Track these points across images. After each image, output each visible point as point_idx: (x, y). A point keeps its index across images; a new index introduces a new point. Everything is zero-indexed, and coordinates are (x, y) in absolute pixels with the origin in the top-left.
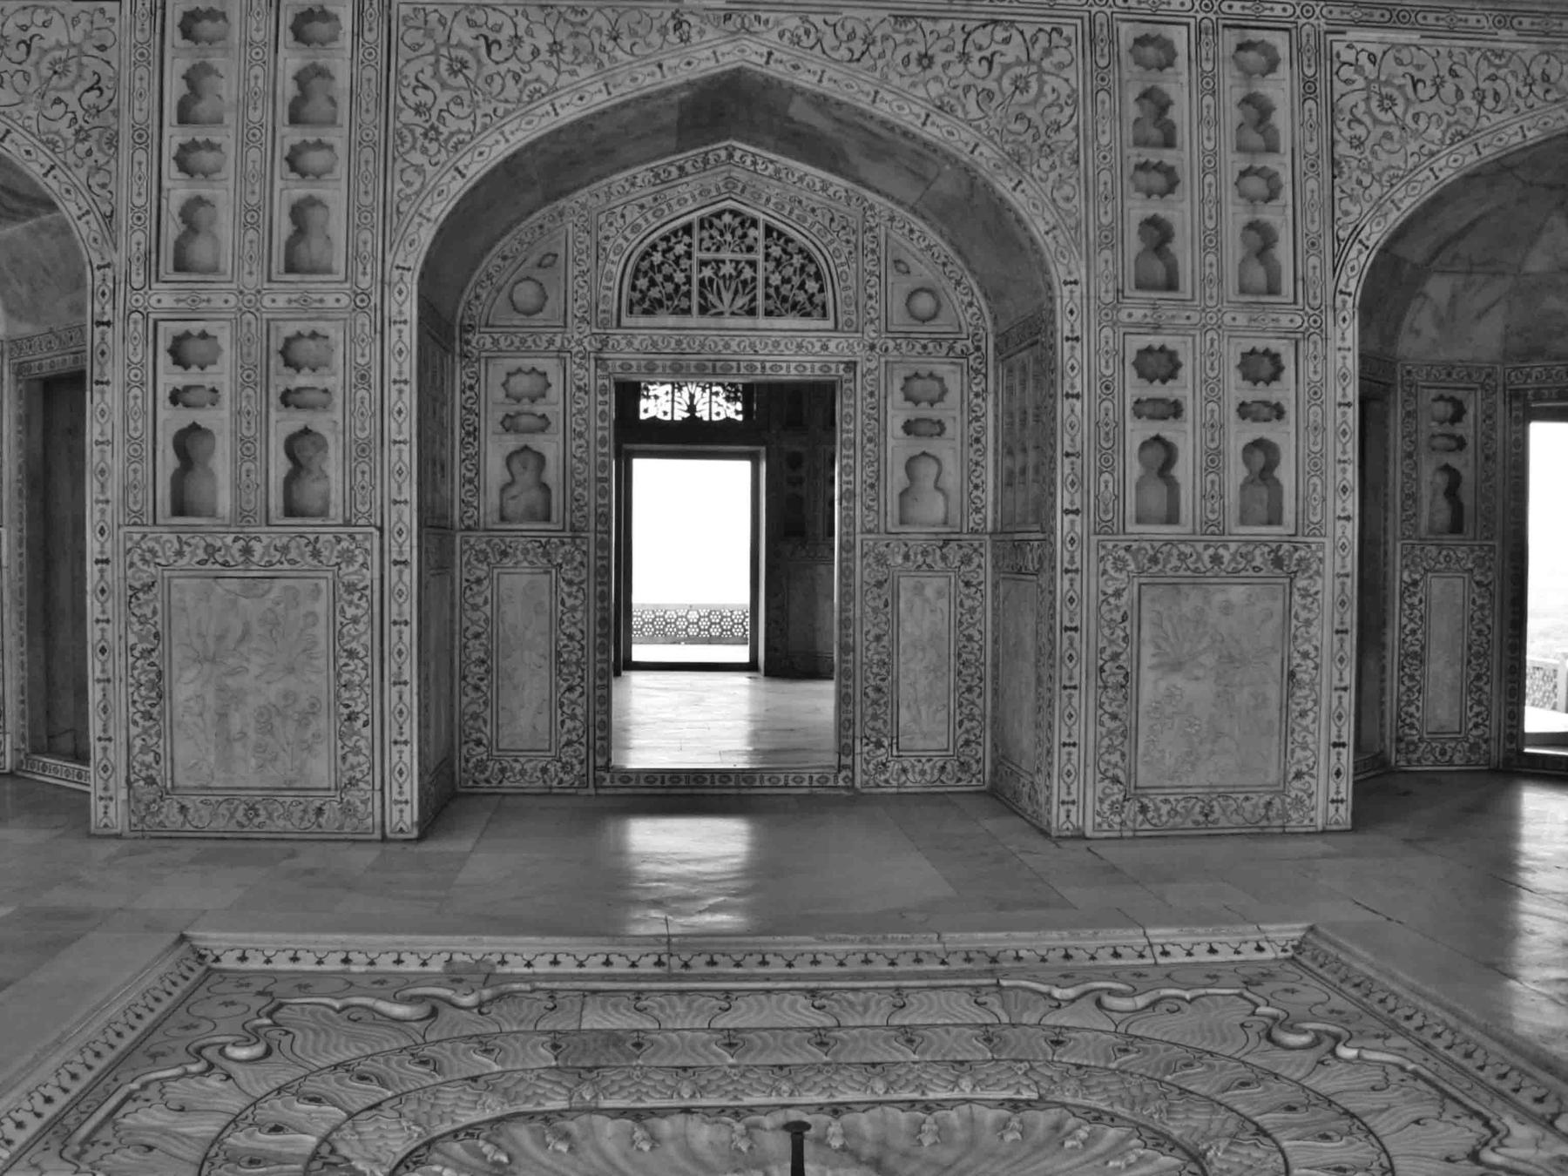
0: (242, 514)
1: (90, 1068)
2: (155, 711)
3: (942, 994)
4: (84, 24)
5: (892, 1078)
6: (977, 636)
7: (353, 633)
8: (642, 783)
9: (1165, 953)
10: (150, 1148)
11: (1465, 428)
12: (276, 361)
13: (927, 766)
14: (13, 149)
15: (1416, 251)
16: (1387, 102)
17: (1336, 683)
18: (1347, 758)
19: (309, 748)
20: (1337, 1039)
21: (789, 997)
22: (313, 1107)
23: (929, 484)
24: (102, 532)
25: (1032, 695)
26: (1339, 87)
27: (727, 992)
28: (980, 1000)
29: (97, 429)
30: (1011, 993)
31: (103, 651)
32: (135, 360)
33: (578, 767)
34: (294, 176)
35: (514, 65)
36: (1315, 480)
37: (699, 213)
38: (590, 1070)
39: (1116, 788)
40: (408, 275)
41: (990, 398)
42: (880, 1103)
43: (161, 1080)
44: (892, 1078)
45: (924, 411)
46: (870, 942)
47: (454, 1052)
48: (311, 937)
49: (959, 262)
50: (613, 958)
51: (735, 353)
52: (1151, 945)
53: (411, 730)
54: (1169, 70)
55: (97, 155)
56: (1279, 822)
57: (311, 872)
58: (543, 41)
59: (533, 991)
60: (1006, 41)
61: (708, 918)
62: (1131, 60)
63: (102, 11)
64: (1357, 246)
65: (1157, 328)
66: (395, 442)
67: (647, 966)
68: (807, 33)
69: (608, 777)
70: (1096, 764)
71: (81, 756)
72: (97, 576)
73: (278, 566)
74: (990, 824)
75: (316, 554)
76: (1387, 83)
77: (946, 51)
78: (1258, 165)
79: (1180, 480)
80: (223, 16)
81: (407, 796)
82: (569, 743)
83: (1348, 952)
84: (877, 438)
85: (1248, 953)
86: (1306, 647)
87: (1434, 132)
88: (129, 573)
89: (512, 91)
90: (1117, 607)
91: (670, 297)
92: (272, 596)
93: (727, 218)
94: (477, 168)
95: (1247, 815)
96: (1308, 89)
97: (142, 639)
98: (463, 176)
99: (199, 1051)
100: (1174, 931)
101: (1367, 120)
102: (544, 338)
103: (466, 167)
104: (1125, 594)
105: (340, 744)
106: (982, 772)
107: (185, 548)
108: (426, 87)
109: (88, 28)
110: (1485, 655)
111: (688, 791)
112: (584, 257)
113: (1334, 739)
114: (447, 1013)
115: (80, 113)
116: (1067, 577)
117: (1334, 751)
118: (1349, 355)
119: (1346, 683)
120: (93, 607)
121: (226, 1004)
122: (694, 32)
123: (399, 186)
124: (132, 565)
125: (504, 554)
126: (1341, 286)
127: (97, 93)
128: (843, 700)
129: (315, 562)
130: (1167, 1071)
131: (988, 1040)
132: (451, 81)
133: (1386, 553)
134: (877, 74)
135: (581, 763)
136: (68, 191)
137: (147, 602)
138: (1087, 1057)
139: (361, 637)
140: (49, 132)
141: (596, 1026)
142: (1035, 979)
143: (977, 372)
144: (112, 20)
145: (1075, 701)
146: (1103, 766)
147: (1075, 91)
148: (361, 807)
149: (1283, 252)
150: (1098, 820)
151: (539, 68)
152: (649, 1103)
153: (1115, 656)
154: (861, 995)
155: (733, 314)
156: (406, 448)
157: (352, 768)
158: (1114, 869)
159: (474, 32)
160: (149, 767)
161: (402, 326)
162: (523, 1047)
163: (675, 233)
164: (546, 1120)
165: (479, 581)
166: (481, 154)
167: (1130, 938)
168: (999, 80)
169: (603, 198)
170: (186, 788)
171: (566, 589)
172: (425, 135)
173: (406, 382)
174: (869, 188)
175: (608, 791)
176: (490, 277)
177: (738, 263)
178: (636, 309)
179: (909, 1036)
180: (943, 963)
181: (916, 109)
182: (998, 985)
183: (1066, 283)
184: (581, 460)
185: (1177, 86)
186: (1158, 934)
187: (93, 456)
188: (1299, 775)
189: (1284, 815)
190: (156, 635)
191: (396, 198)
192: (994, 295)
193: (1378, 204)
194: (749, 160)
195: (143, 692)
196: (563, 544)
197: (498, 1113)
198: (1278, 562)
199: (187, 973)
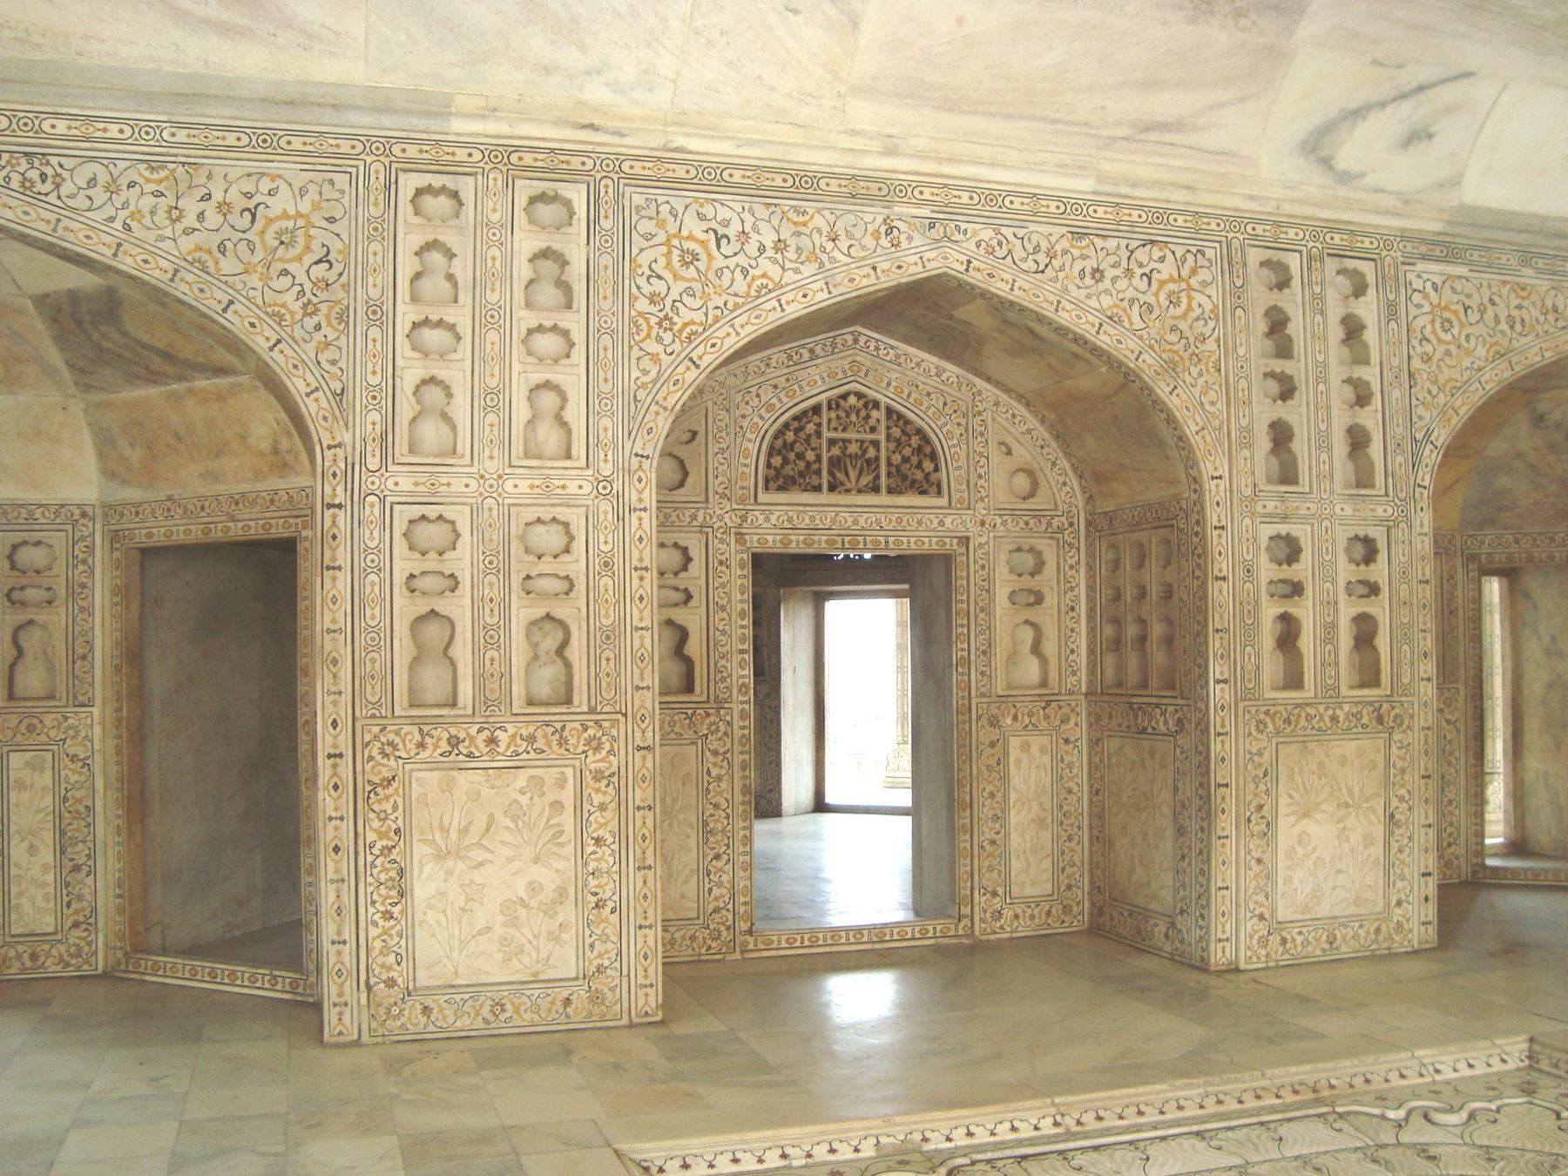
0: (485, 702)
7: (601, 820)
8: (784, 945)
13: (1036, 911)
14: (236, 322)
16: (1447, 325)
17: (1423, 821)
19: (554, 938)
24: (334, 724)
25: (1168, 845)
26: (1413, 311)
31: (336, 849)
33: (724, 933)
35: (741, 260)
37: (828, 394)
40: (646, 464)
41: (1083, 570)
48: (737, 1137)
49: (1054, 445)
51: (863, 529)
54: (1286, 291)
55: (326, 330)
58: (769, 238)
60: (1162, 259)
63: (332, 182)
65: (1285, 518)
66: (637, 629)
68: (1000, 244)
69: (751, 940)
70: (1247, 904)
72: (329, 772)
73: (524, 756)
75: (562, 742)
77: (1115, 266)
78: (1355, 376)
79: (1304, 650)
84: (988, 610)
86: (1403, 792)
87: (1481, 352)
88: (368, 767)
89: (741, 285)
90: (1260, 765)
91: (802, 474)
93: (852, 400)
94: (709, 360)
96: (1391, 311)
97: (382, 835)
98: (698, 367)
101: (1433, 339)
102: (688, 513)
103: (700, 358)
104: (1266, 753)
105: (588, 932)
106: (1082, 913)
107: (428, 740)
111: (827, 949)
112: (723, 434)
113: (1423, 870)
115: (308, 286)
116: (1219, 739)
118: (1426, 539)
122: (903, 238)
124: (371, 758)
127: (326, 265)
129: (562, 751)
132: (683, 272)
134: (1059, 285)
135: (728, 928)
136: (295, 367)
137: (387, 798)
143: (1071, 546)
144: (342, 192)
147: (1216, 306)
148: (609, 995)
149: (1375, 450)
151: (765, 265)
155: (860, 491)
156: (647, 634)
157: (600, 956)
160: (390, 969)
161: (642, 514)
163: (804, 413)
166: (713, 345)
168: (1156, 294)
169: (741, 378)
170: (428, 988)
171: (712, 759)
172: (660, 324)
173: (646, 569)
175: (752, 955)
177: (862, 442)
178: (771, 484)
181: (1091, 318)
183: (1213, 478)
184: (723, 632)
185: (1292, 302)
188: (1399, 903)
191: (633, 387)
192: (1095, 478)
193: (1443, 412)
194: (872, 345)
195: (383, 890)
196: (708, 715)
198: (1380, 720)
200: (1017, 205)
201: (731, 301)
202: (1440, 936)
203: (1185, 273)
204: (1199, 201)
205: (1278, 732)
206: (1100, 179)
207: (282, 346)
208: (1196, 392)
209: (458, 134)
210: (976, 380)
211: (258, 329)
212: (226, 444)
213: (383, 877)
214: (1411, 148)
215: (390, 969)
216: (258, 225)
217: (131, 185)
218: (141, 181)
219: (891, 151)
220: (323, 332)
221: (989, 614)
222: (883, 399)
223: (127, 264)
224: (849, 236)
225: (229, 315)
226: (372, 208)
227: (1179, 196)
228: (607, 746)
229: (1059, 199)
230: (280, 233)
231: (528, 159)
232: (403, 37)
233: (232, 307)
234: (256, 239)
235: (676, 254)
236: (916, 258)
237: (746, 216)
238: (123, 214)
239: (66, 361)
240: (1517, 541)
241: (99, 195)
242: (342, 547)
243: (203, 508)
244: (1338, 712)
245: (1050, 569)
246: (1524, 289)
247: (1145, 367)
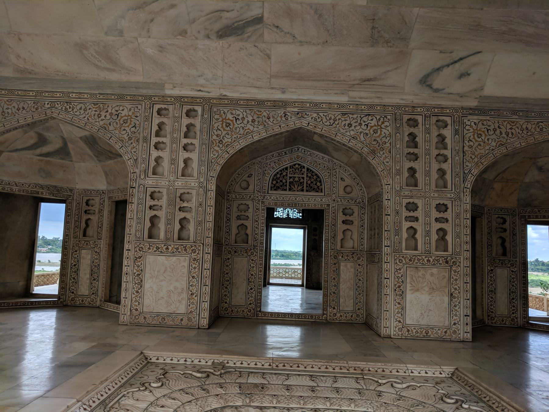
0: (167, 239)
1: (114, 387)
2: (140, 291)
3: (348, 379)
4: (132, 111)
5: (332, 402)
6: (362, 280)
9: (412, 372)
10: (128, 410)
11: (507, 226)
12: (178, 200)
14: (112, 142)
15: (490, 176)
16: (479, 136)
18: (469, 320)
19: (180, 302)
20: (463, 402)
21: (305, 377)
22: (173, 401)
23: (349, 237)
27: (288, 374)
28: (358, 381)
29: (129, 215)
30: (367, 380)
31: (127, 274)
34: (185, 151)
35: (242, 125)
36: (458, 240)
38: (249, 394)
39: (400, 324)
40: (213, 179)
41: (366, 215)
42: (328, 409)
43: (133, 392)
44: (332, 402)
45: (348, 218)
46: (328, 363)
47: (212, 387)
48: (177, 354)
50: (257, 363)
52: (408, 369)
53: (208, 298)
55: (133, 144)
56: (449, 337)
57: (177, 336)
58: (250, 119)
59: (236, 371)
60: (372, 120)
61: (284, 353)
62: (406, 125)
63: (137, 107)
64: (470, 175)
65: (411, 197)
67: (266, 366)
68: (319, 118)
70: (394, 317)
71: (118, 303)
72: (127, 254)
74: (364, 332)
75: (185, 250)
76: (480, 130)
78: (441, 153)
80: (168, 109)
81: (205, 316)
82: (250, 304)
83: (467, 376)
85: (437, 374)
86: (456, 287)
87: (494, 144)
89: (242, 131)
90: (400, 273)
91: (281, 186)
92: (173, 260)
93: (297, 166)
94: (232, 152)
95: (439, 335)
96: (456, 132)
97: (137, 271)
99: (143, 384)
100: (415, 366)
101: (473, 140)
108: (219, 130)
110: (515, 292)
113: (465, 314)
114: (212, 376)
116: (386, 264)
117: (465, 317)
118: (468, 205)
119: (468, 298)
120: (125, 262)
121: (152, 372)
122: (289, 117)
123: (212, 155)
124: (136, 251)
125: (235, 252)
126: (465, 186)
128: (325, 296)
130: (412, 406)
131: (360, 393)
132: (226, 129)
133: (482, 261)
137: (140, 261)
138: (388, 400)
139: (196, 272)
141: (252, 382)
142: (373, 376)
145: (388, 299)
146: (396, 318)
147: (390, 133)
149: (448, 177)
150: (395, 333)
152: (265, 405)
153: (399, 287)
154: (325, 378)
157: (191, 308)
158: (398, 347)
159: (232, 116)
160: (137, 306)
162: (231, 386)
163: (283, 169)
164: (236, 408)
165: (228, 259)
167: (402, 367)
168: (369, 130)
172: (219, 142)
174: (334, 158)
176: (235, 179)
179: (337, 390)
180: (348, 370)
181: (347, 138)
182: (363, 377)
184: (257, 228)
185: (419, 131)
186: (410, 366)
187: (128, 222)
188: (455, 324)
189: (451, 335)
190: (141, 270)
192: (368, 187)
193: (477, 164)
195: (137, 285)
197: (223, 405)
199: (142, 362)
200: (324, 106)
201: (239, 136)
202: (472, 337)
203: (380, 123)
204: (384, 101)
205: (407, 263)
206: (349, 97)
208: (382, 159)
210: (334, 160)
213: (137, 282)
214: (462, 79)
215: (137, 306)
217: (90, 109)
219: (284, 92)
221: (335, 226)
222: (306, 166)
224: (273, 117)
225: (111, 140)
227: (377, 101)
228: (197, 252)
229: (338, 104)
230: (124, 120)
231: (186, 100)
234: (118, 122)
235: (224, 123)
236: (293, 123)
237: (244, 113)
238: (87, 116)
240: (539, 211)
241: (82, 111)
244: (430, 259)
245: (356, 214)
246: (513, 123)
247: (364, 152)
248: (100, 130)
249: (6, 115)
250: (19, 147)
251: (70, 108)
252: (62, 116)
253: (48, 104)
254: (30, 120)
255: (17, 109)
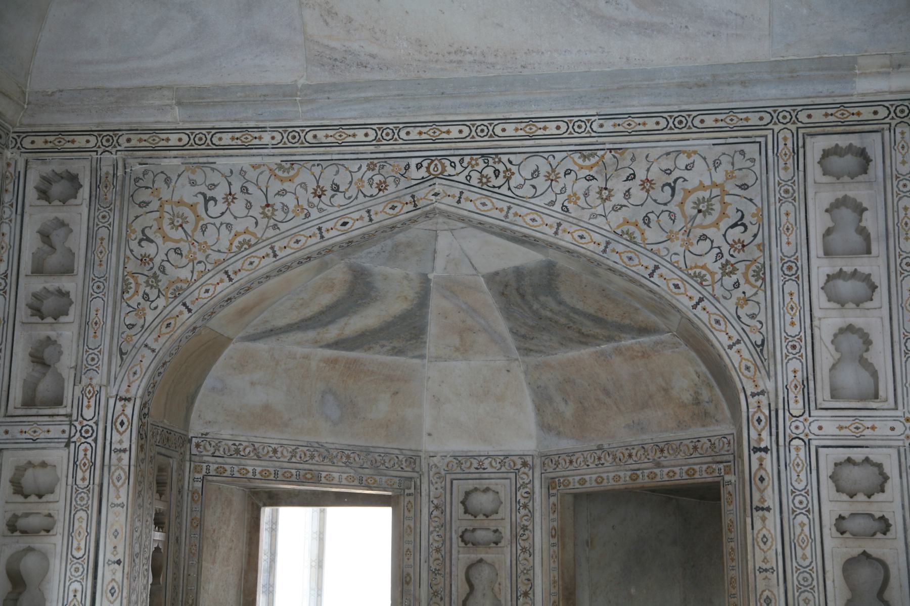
14: (662, 284)
32: (800, 486)
55: (744, 287)
63: (742, 153)
109: (730, 168)
115: (725, 249)
127: (742, 228)
136: (717, 322)
140: (696, 267)
144: (753, 160)
207: (705, 303)
209: (864, 95)
211: (682, 290)
212: (651, 397)
216: (678, 198)
217: (568, 172)
218: (576, 168)
220: (741, 289)
223: (566, 240)
225: (655, 278)
226: (782, 172)
230: (697, 203)
232: (805, 11)
233: (658, 272)
238: (561, 198)
239: (511, 330)
241: (541, 183)
242: (770, 489)
243: (630, 456)
248: (610, 247)
249: (280, 215)
250: (281, 322)
251: (497, 173)
252: (470, 206)
253: (419, 166)
254: (358, 227)
255: (315, 193)
